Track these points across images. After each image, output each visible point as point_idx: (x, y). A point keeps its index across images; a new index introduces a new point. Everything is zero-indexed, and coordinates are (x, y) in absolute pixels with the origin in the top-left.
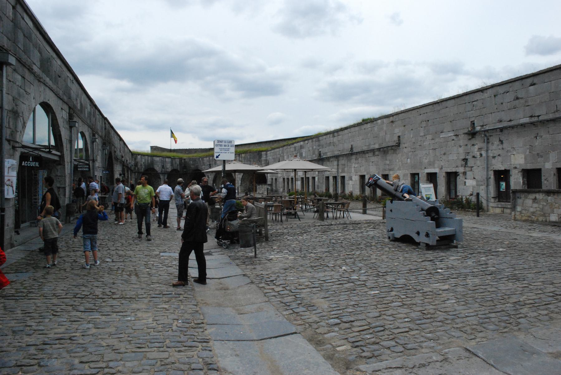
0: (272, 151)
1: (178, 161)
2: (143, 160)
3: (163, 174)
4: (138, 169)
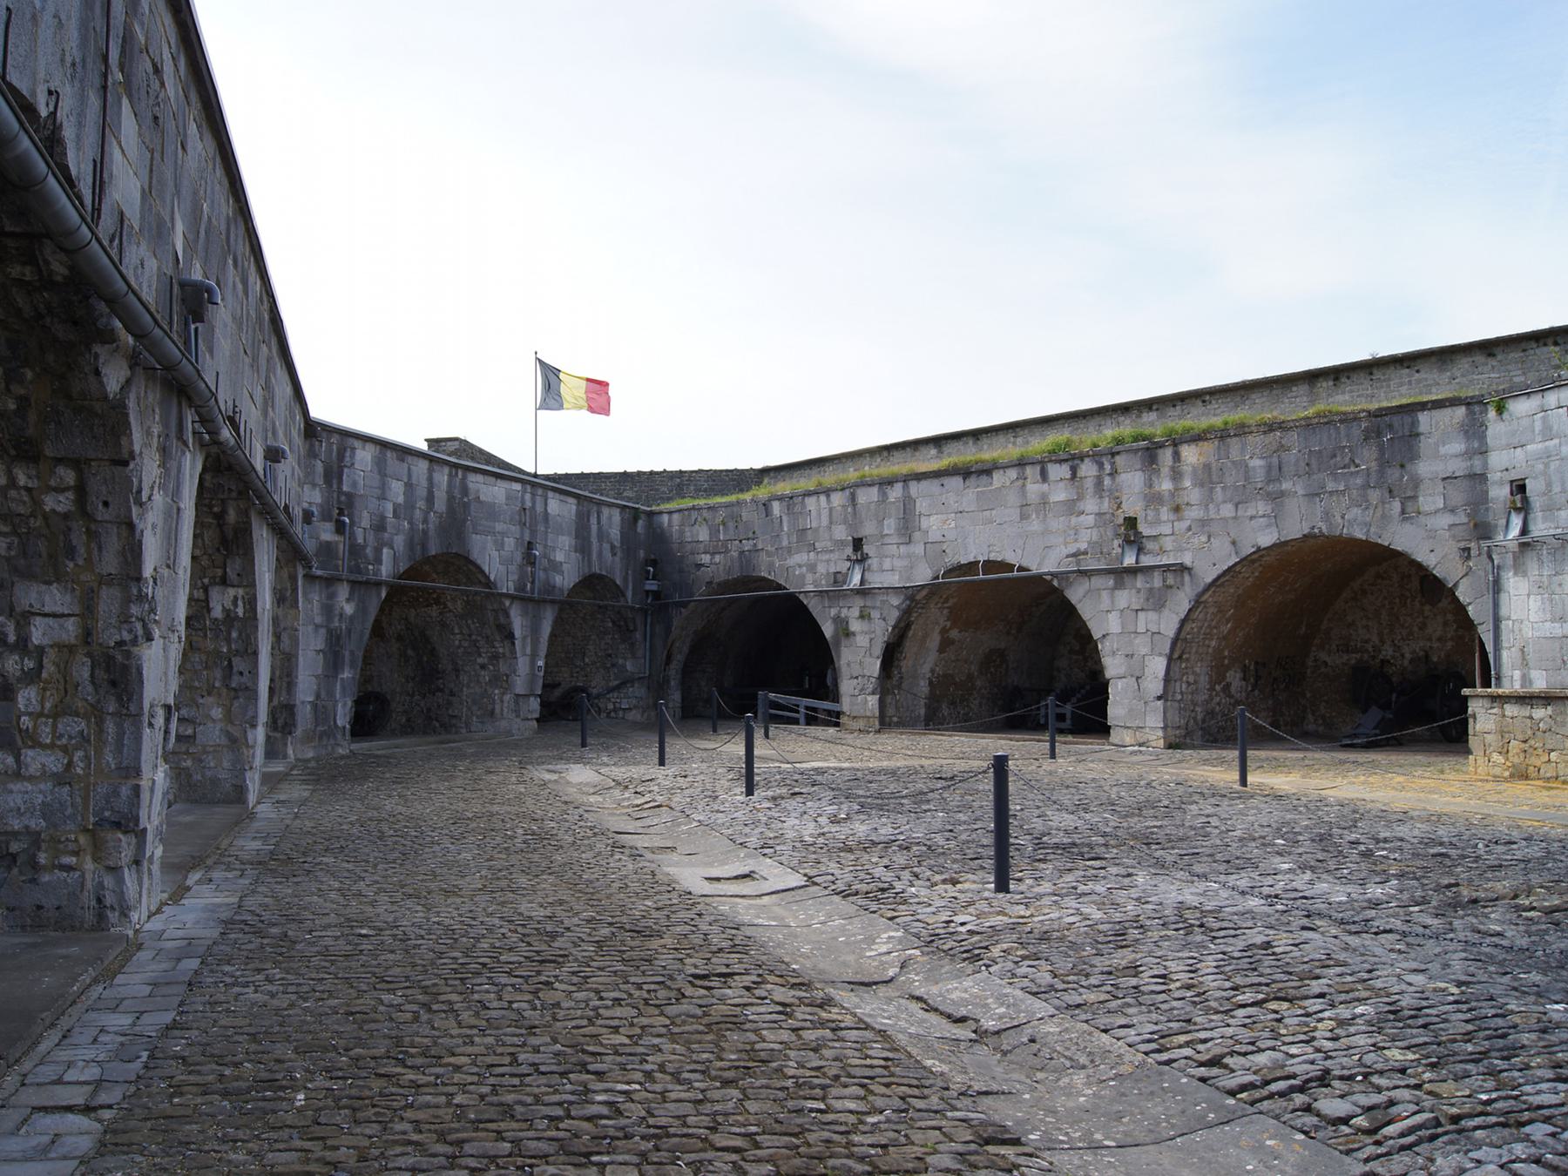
1: (613, 521)
2: (397, 489)
3: (531, 600)
4: (355, 550)
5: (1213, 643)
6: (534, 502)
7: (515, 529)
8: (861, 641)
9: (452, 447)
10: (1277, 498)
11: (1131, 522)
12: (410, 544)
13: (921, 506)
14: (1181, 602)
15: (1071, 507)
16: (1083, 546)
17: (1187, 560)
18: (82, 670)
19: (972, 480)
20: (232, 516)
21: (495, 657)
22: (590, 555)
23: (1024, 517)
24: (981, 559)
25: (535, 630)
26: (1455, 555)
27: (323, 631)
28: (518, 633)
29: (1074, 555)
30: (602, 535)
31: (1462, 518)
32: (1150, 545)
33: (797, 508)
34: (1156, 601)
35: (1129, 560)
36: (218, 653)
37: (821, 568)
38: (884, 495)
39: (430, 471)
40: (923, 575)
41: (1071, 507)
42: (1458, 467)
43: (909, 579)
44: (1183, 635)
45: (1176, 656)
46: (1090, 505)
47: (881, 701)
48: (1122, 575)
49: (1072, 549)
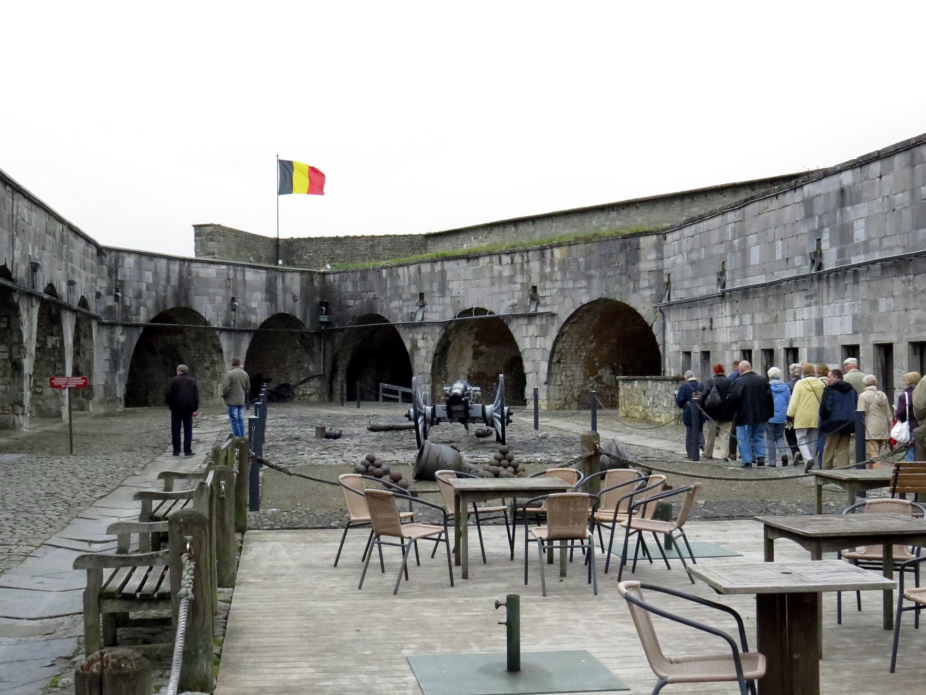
0: (688, 231)
2: (149, 276)
4: (126, 309)
5: (584, 354)
6: (235, 276)
7: (223, 291)
8: (423, 353)
9: (209, 229)
10: (589, 278)
11: (535, 288)
12: (157, 302)
13: (449, 276)
14: (554, 333)
15: (511, 280)
16: (516, 301)
17: (555, 311)
18: (9, 365)
19: (471, 262)
20: (54, 311)
21: (213, 363)
22: (276, 302)
23: (493, 284)
24: (475, 307)
25: (237, 348)
26: (651, 311)
27: (108, 350)
28: (225, 349)
29: (513, 306)
30: (285, 290)
31: (654, 292)
32: (542, 302)
33: (394, 274)
34: (544, 333)
35: (532, 310)
36: (50, 361)
37: (405, 310)
38: (433, 268)
39: (168, 264)
40: (450, 316)
41: (511, 280)
42: (652, 266)
43: (444, 317)
44: (557, 350)
45: (554, 360)
46: (519, 279)
47: (432, 387)
48: (531, 317)
49: (511, 302)
